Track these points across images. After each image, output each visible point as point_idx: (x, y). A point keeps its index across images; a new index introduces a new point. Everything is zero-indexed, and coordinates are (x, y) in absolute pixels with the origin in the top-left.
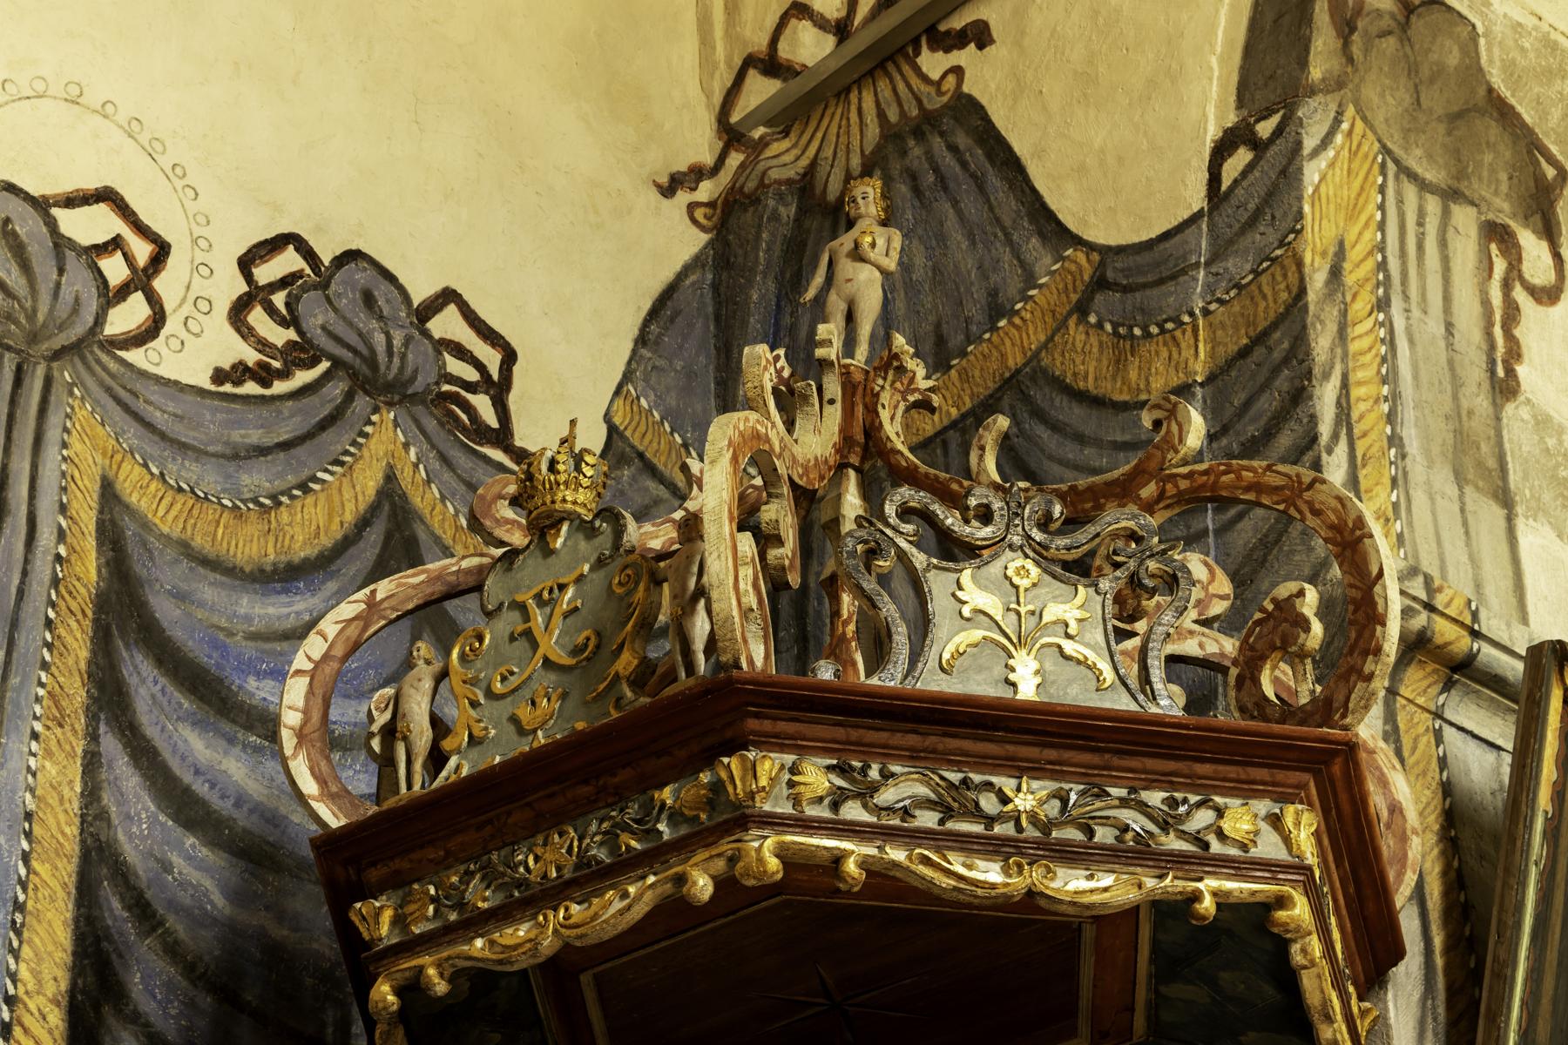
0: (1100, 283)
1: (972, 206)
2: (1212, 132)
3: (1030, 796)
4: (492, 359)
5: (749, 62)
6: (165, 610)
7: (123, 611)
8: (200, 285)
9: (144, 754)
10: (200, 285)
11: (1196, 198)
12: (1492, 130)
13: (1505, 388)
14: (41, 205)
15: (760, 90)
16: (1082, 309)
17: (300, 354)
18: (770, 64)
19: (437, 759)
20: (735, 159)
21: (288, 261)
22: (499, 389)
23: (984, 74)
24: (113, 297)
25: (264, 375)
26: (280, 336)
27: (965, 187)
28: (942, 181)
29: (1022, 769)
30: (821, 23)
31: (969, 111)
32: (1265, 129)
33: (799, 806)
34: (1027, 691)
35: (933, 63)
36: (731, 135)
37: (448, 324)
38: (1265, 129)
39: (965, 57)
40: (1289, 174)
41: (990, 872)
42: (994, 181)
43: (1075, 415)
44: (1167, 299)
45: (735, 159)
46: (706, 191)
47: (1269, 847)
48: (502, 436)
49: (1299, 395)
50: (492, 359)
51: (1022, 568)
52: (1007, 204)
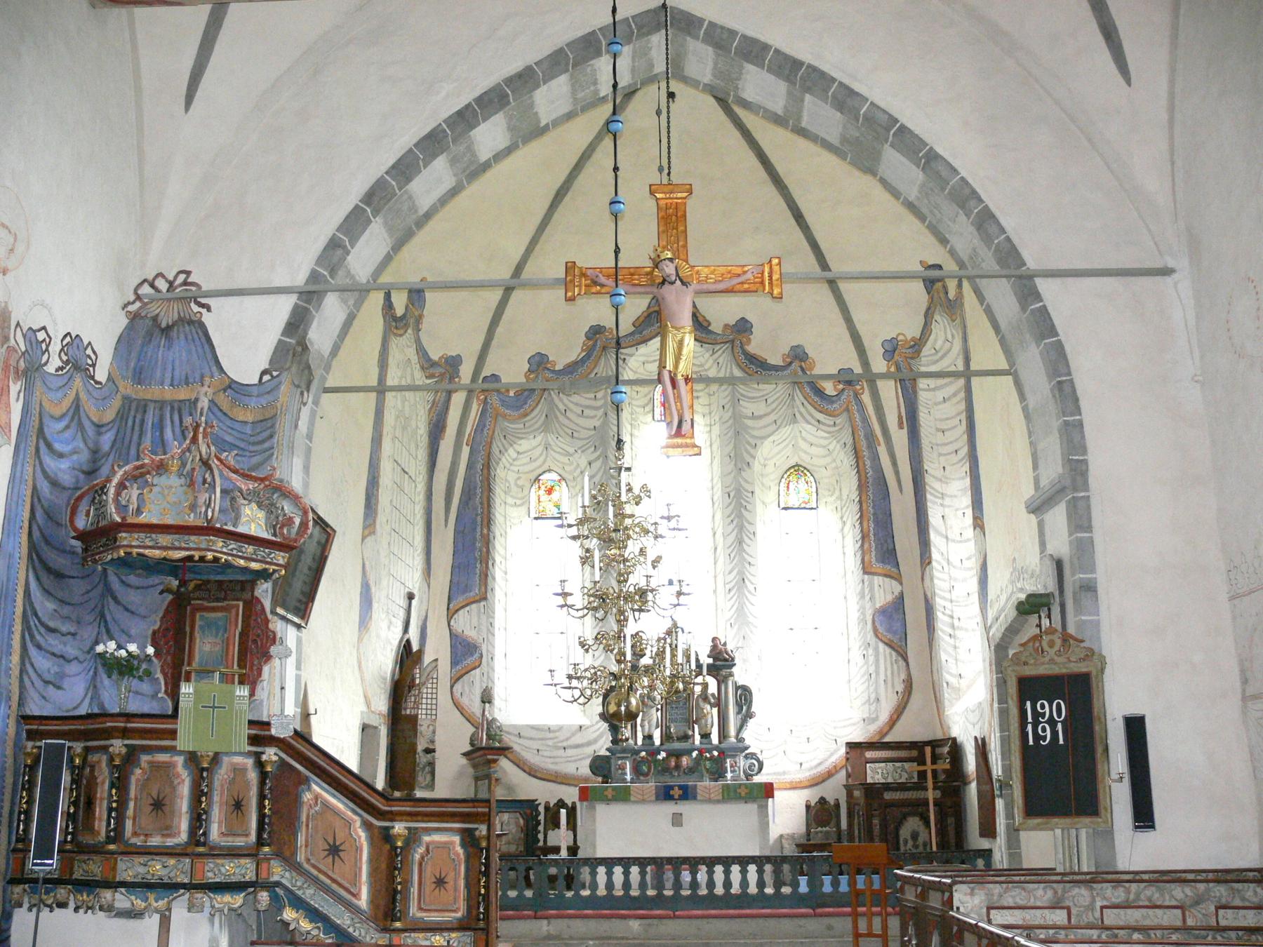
0: (230, 387)
1: (200, 350)
2: (263, 368)
3: (250, 549)
4: (93, 357)
5: (145, 281)
6: (46, 430)
7: (41, 432)
8: (55, 347)
9: (41, 463)
10: (55, 347)
11: (256, 381)
12: (306, 372)
13: (296, 426)
14: (35, 331)
15: (146, 289)
16: (225, 390)
17: (67, 363)
18: (152, 286)
19: (139, 511)
20: (138, 304)
21: (68, 339)
22: (94, 365)
23: (207, 318)
24: (43, 353)
25: (61, 368)
26: (65, 358)
27: (198, 342)
28: (193, 340)
29: (249, 544)
30: (167, 280)
31: (202, 326)
32: (275, 374)
33: (219, 548)
34: (253, 532)
35: (195, 308)
36: (138, 298)
37: (89, 351)
38: (275, 374)
39: (204, 311)
40: (278, 386)
41: (242, 562)
42: (206, 346)
43: (219, 414)
44: (246, 399)
45: (138, 304)
46: (131, 308)
47: (281, 562)
48: (92, 378)
49: (271, 436)
50: (93, 357)
51: (254, 506)
52: (209, 356)
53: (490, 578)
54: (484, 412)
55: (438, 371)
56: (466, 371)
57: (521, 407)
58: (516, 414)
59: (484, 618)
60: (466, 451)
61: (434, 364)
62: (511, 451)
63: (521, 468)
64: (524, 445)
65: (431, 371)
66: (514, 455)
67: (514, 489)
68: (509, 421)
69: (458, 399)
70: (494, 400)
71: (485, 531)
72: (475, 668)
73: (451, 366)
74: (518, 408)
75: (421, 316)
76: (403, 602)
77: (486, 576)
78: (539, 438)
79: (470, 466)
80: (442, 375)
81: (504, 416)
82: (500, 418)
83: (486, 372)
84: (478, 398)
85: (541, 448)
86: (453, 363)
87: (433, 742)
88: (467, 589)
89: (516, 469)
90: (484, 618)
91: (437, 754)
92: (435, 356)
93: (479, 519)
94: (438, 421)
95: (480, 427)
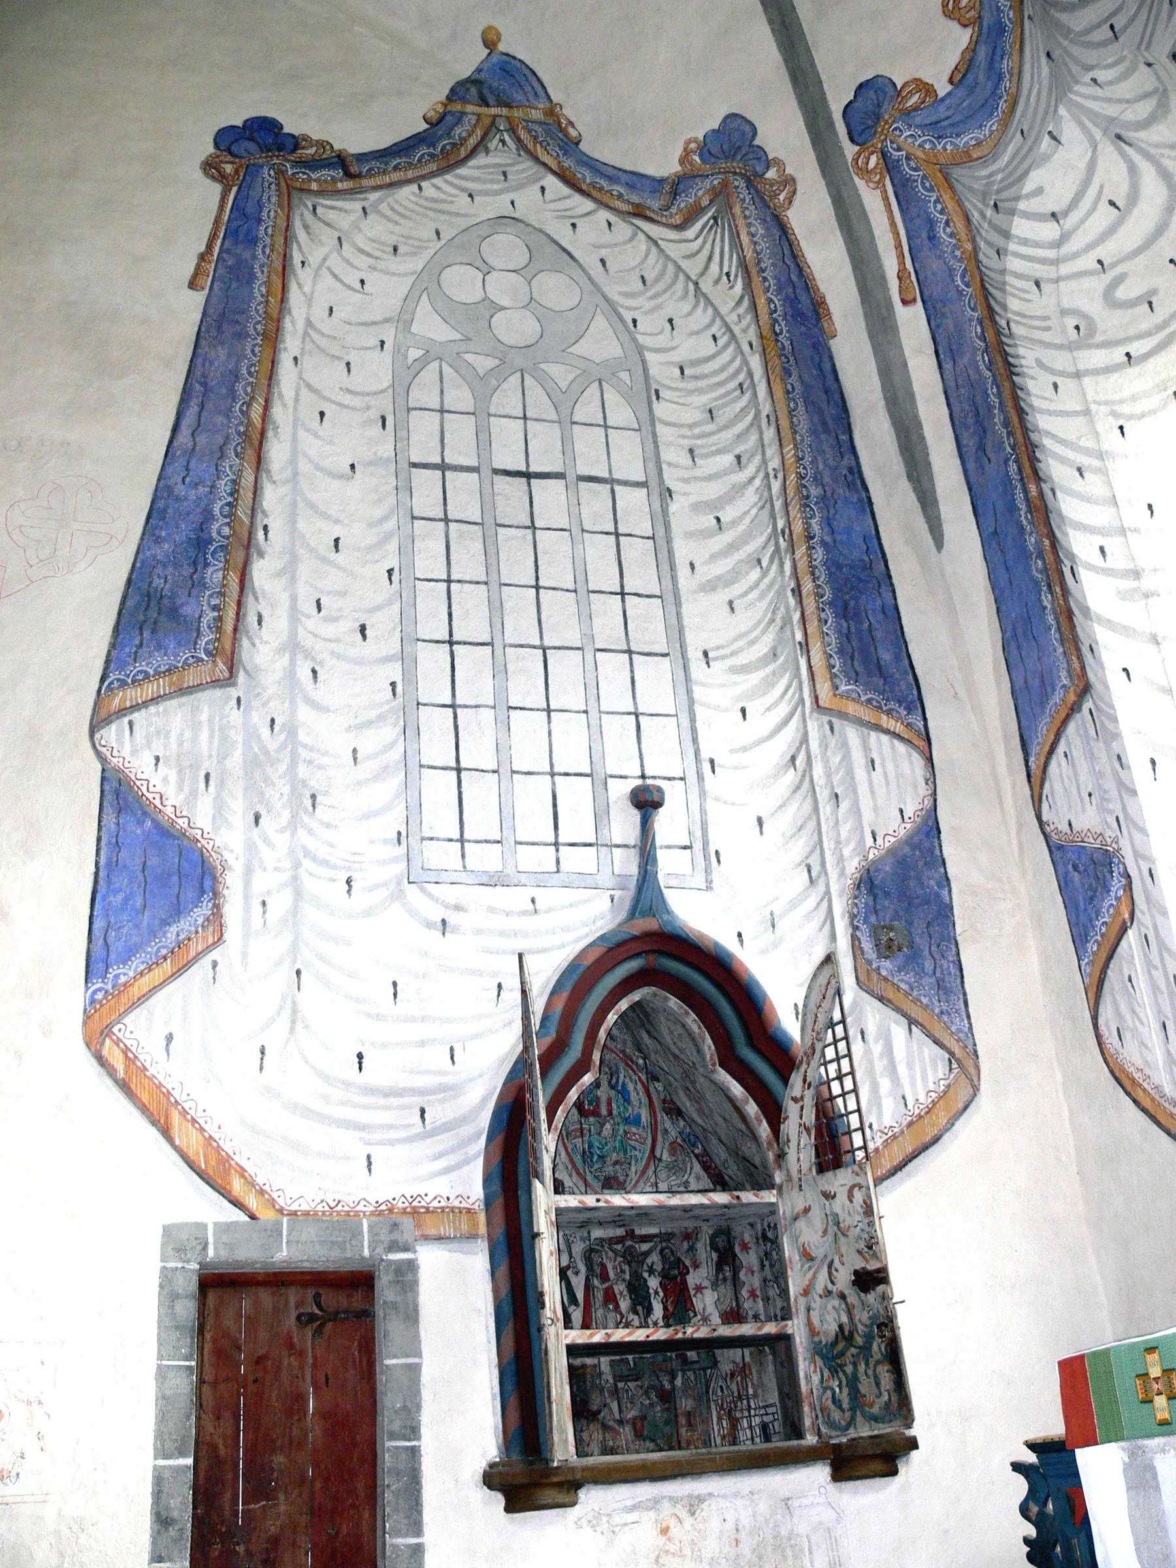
53: (1078, 618)
54: (905, 194)
55: (700, 192)
56: (783, 135)
57: (995, 95)
58: (992, 125)
59: (1099, 748)
60: (912, 322)
61: (675, 186)
62: (1020, 227)
63: (1106, 252)
64: (1053, 179)
65: (683, 202)
66: (1050, 231)
67: (1109, 322)
68: (984, 160)
69: (811, 217)
70: (909, 141)
71: (1033, 488)
72: (1123, 930)
73: (729, 155)
74: (987, 107)
75: (552, 111)
76: (624, 825)
77: (1070, 615)
78: (1070, 130)
79: (945, 350)
80: (716, 194)
81: (966, 158)
82: (957, 173)
83: (838, 98)
84: (864, 172)
85: (1108, 154)
86: (732, 150)
87: (872, 1245)
88: (1046, 684)
89: (1088, 262)
90: (1099, 748)
91: (900, 1284)
92: (665, 164)
93: (1013, 467)
94: (792, 302)
95: (921, 234)
